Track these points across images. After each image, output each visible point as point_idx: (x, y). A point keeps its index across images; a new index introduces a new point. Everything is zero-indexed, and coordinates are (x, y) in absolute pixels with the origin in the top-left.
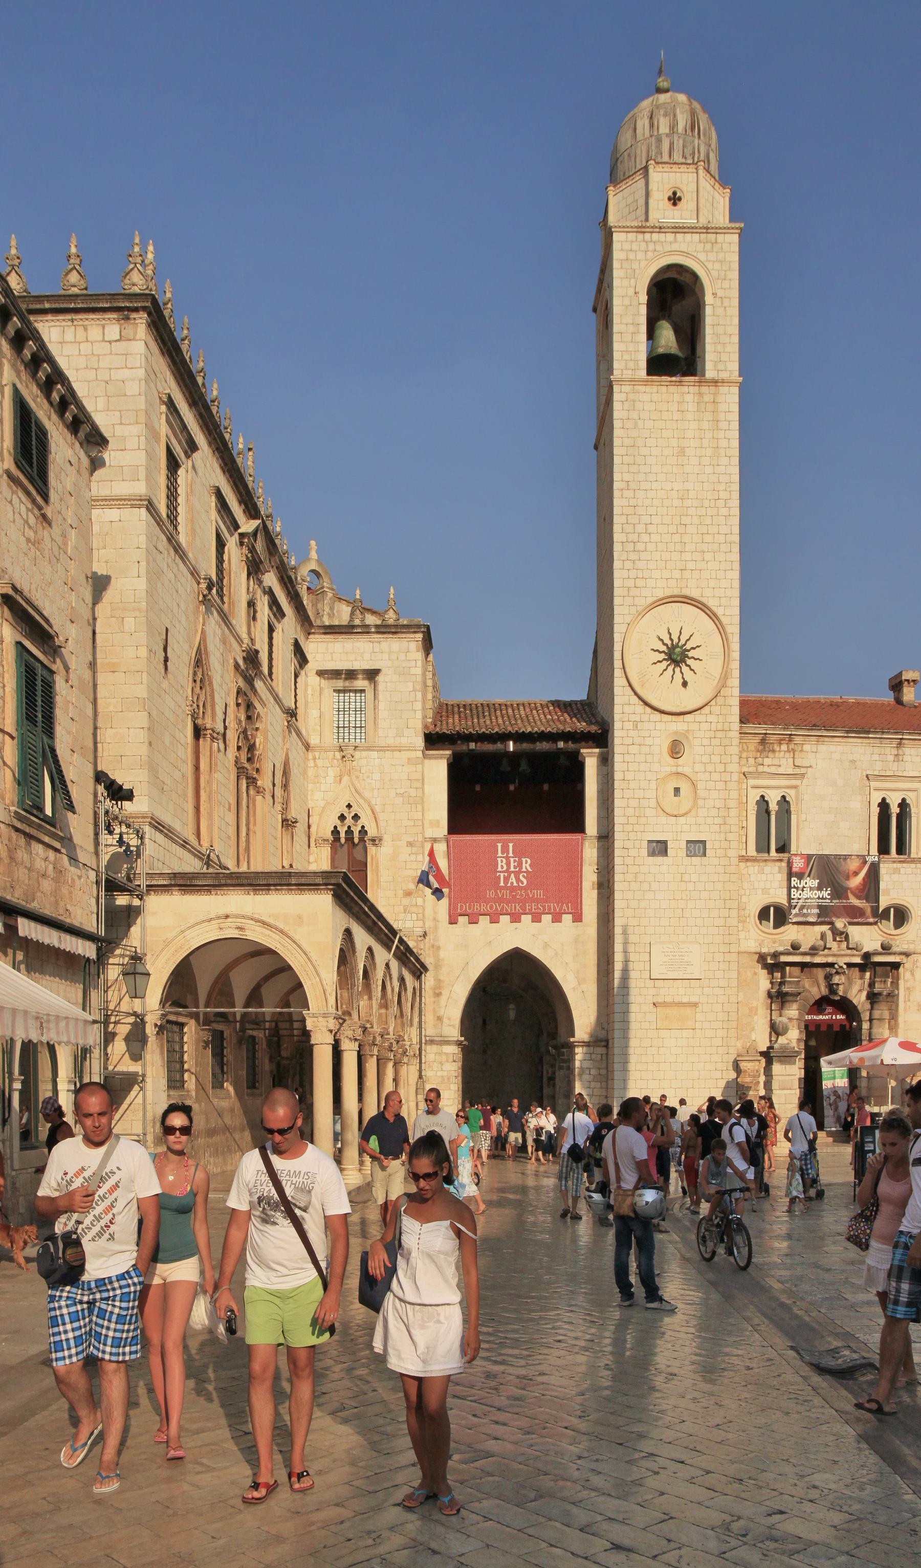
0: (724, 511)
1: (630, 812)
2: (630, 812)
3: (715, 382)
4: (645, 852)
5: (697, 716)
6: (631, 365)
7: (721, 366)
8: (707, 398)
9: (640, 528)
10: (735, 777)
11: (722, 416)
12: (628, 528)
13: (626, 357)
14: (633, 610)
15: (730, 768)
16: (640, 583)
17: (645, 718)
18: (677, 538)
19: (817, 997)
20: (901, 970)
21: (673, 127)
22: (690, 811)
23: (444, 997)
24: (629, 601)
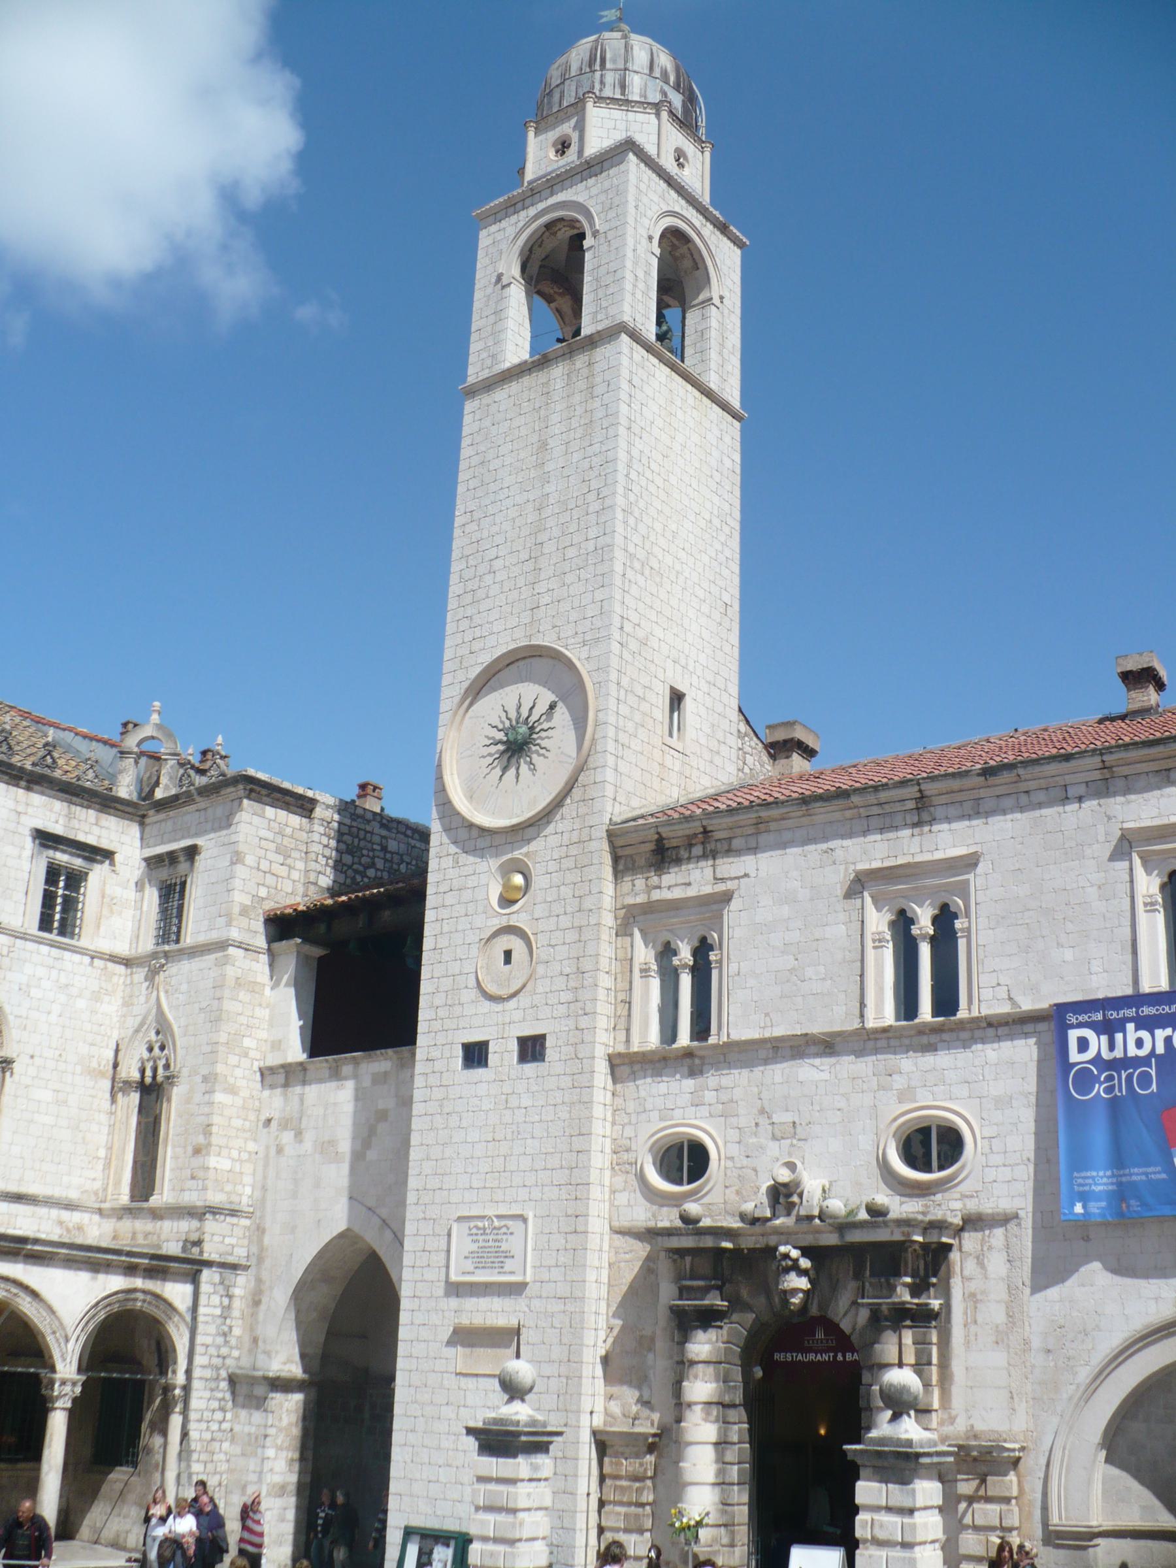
1: (439, 1000)
9: (482, 569)
12: (468, 574)
14: (466, 685)
16: (477, 646)
18: (529, 566)
20: (954, 1256)
22: (524, 986)
23: (263, 1307)
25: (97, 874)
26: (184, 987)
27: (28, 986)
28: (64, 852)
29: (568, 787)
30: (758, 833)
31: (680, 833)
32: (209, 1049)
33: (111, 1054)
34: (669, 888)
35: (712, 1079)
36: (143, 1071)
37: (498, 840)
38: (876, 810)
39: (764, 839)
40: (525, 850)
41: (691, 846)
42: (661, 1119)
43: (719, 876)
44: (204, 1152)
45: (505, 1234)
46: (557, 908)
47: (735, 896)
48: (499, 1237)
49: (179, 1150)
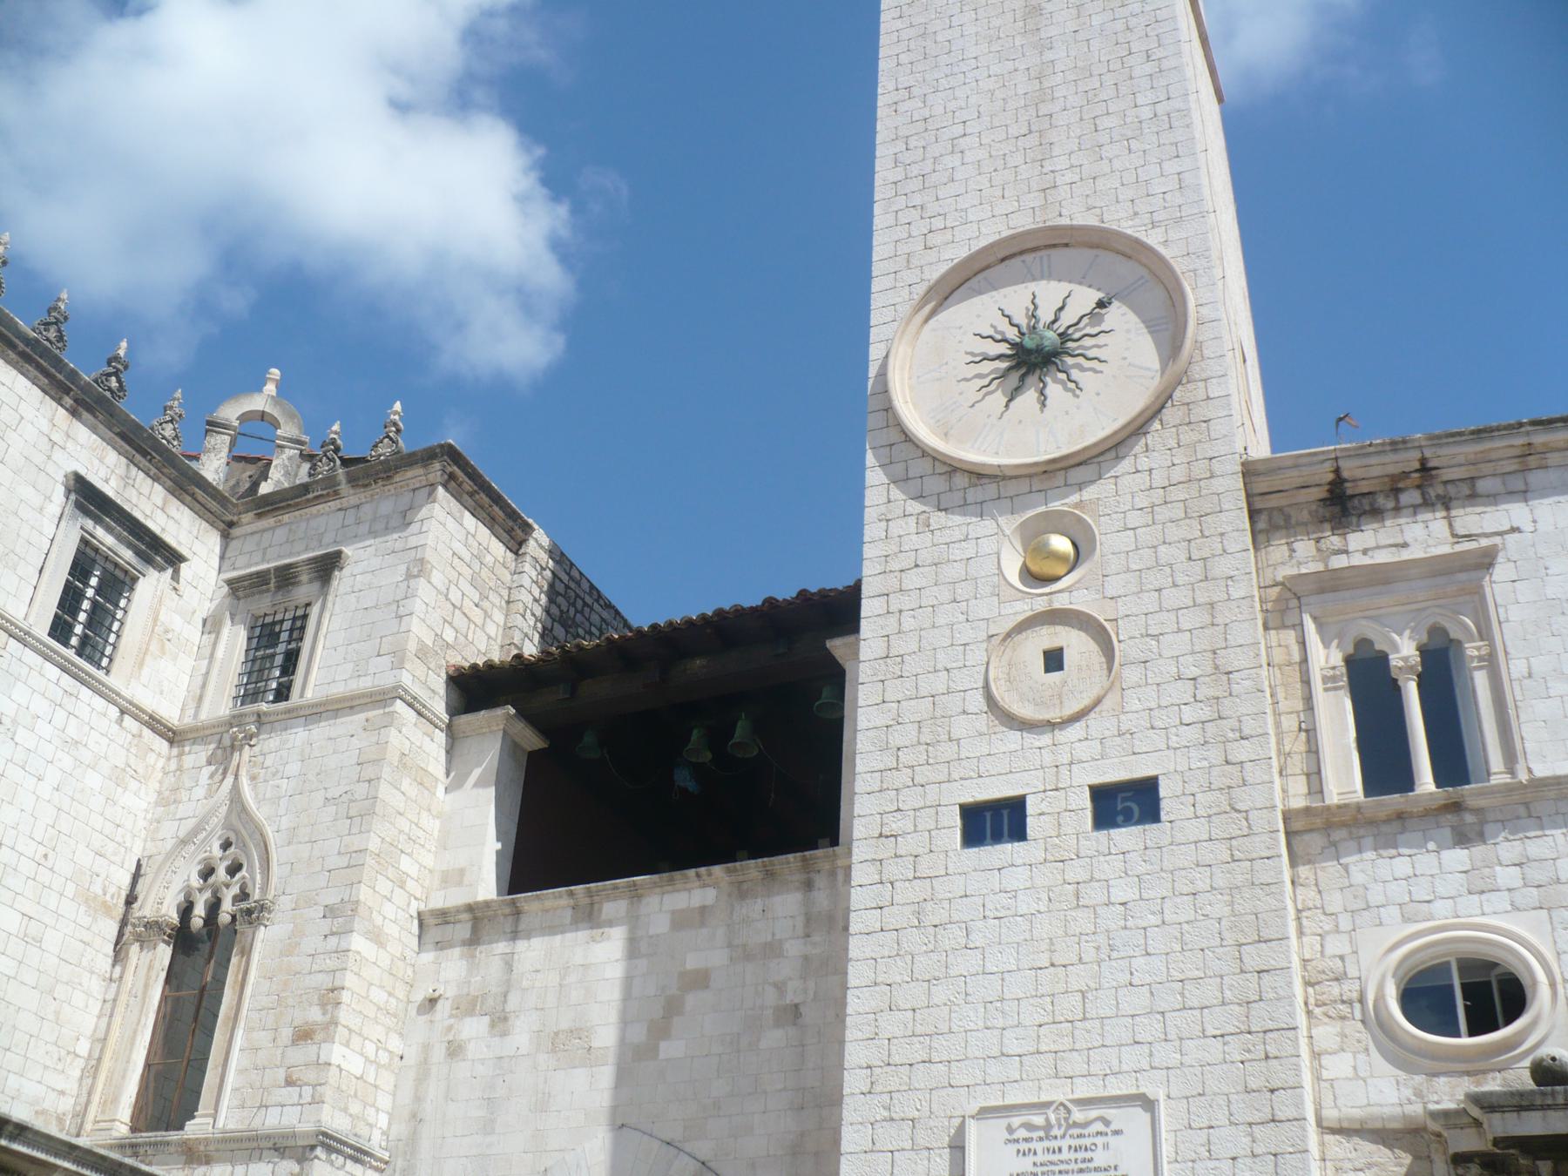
0: (1149, 68)
14: (921, 290)
15: (1222, 567)
16: (934, 239)
18: (1033, 140)
22: (1098, 702)
25: (151, 585)
26: (293, 768)
27: (14, 721)
28: (109, 529)
29: (1157, 406)
30: (1526, 470)
31: (1376, 471)
32: (344, 861)
33: (126, 880)
34: (1365, 552)
35: (1507, 848)
36: (186, 911)
37: (1011, 488)
39: (1535, 478)
40: (1075, 498)
41: (1394, 487)
42: (1407, 920)
43: (1461, 532)
44: (318, 1037)
45: (1099, 1133)
46: (1155, 579)
47: (1500, 558)
48: (1087, 1142)
49: (263, 1038)
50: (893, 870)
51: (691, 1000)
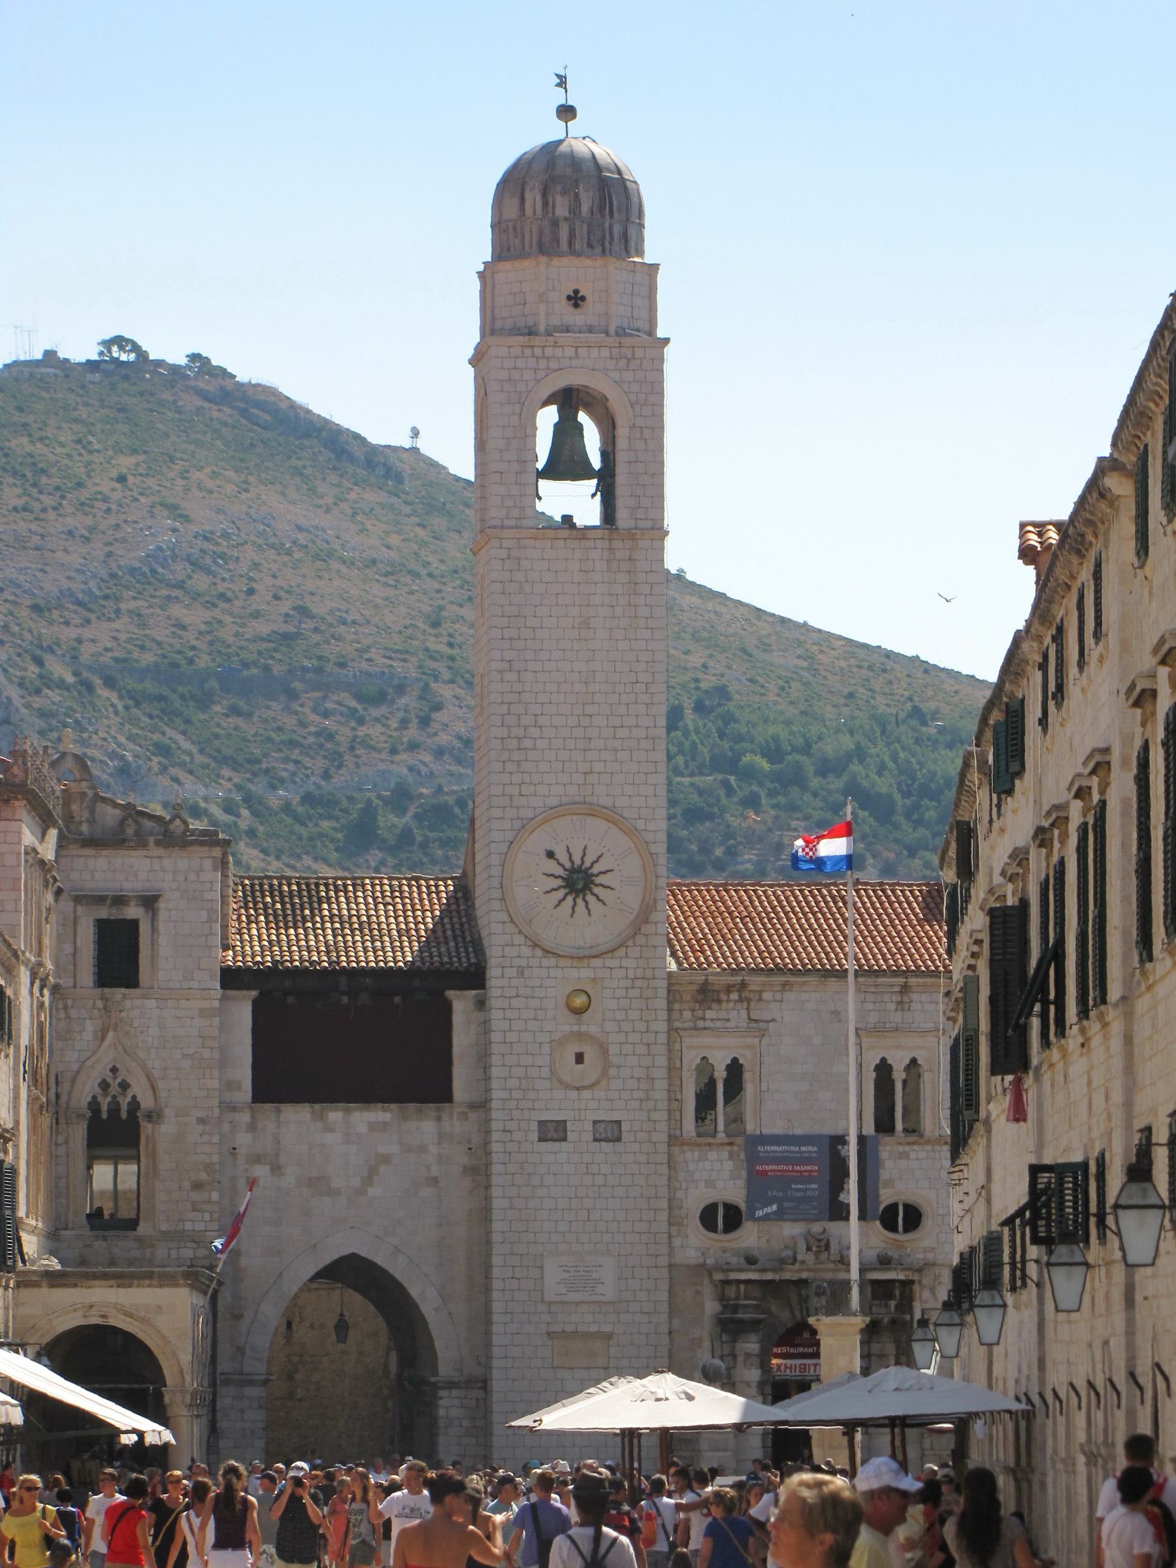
1: (512, 1083)
2: (512, 1083)
3: (632, 535)
4: (535, 1136)
5: (609, 962)
6: (515, 513)
7: (640, 514)
8: (620, 555)
10: (662, 1038)
11: (642, 577)
13: (509, 502)
15: (655, 1026)
17: (534, 962)
18: (578, 732)
19: (790, 1325)
20: (916, 1287)
21: (575, 209)
22: (597, 1082)
24: (511, 813)
30: (783, 991)
36: (94, 1106)
37: (563, 962)
38: (873, 989)
43: (752, 1017)
50: (512, 1147)
51: (382, 1169)
